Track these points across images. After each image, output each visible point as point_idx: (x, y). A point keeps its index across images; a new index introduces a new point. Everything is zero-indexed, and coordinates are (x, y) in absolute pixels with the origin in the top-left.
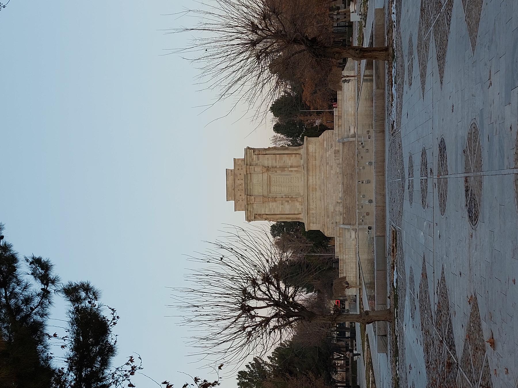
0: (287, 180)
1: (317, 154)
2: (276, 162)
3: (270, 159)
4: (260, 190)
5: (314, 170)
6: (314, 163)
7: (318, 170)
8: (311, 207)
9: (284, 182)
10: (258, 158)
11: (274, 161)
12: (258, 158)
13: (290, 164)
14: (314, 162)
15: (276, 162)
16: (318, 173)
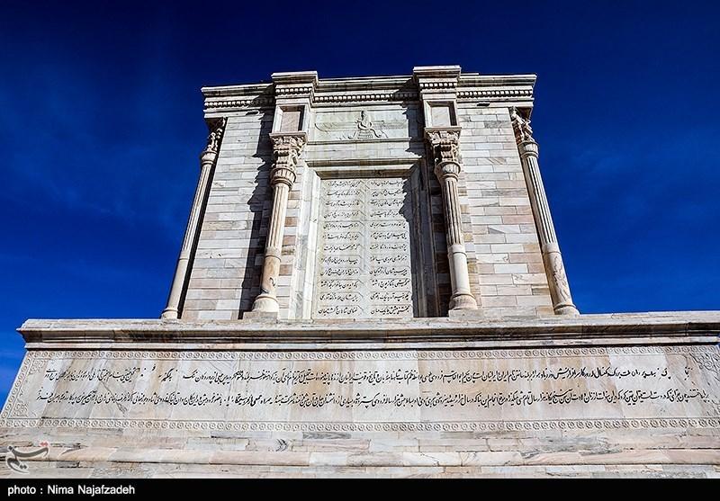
0: (389, 253)
1: (598, 410)
2: (487, 193)
3: (499, 168)
4: (335, 135)
5: (469, 390)
6: (523, 386)
7: (471, 415)
8: (185, 364)
9: (376, 236)
10: (498, 124)
11: (492, 185)
12: (498, 124)
13: (483, 259)
14: (537, 386)
15: (487, 193)
16: (437, 415)
